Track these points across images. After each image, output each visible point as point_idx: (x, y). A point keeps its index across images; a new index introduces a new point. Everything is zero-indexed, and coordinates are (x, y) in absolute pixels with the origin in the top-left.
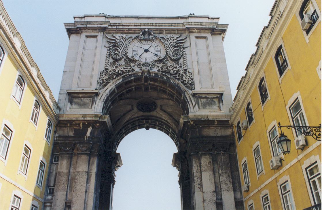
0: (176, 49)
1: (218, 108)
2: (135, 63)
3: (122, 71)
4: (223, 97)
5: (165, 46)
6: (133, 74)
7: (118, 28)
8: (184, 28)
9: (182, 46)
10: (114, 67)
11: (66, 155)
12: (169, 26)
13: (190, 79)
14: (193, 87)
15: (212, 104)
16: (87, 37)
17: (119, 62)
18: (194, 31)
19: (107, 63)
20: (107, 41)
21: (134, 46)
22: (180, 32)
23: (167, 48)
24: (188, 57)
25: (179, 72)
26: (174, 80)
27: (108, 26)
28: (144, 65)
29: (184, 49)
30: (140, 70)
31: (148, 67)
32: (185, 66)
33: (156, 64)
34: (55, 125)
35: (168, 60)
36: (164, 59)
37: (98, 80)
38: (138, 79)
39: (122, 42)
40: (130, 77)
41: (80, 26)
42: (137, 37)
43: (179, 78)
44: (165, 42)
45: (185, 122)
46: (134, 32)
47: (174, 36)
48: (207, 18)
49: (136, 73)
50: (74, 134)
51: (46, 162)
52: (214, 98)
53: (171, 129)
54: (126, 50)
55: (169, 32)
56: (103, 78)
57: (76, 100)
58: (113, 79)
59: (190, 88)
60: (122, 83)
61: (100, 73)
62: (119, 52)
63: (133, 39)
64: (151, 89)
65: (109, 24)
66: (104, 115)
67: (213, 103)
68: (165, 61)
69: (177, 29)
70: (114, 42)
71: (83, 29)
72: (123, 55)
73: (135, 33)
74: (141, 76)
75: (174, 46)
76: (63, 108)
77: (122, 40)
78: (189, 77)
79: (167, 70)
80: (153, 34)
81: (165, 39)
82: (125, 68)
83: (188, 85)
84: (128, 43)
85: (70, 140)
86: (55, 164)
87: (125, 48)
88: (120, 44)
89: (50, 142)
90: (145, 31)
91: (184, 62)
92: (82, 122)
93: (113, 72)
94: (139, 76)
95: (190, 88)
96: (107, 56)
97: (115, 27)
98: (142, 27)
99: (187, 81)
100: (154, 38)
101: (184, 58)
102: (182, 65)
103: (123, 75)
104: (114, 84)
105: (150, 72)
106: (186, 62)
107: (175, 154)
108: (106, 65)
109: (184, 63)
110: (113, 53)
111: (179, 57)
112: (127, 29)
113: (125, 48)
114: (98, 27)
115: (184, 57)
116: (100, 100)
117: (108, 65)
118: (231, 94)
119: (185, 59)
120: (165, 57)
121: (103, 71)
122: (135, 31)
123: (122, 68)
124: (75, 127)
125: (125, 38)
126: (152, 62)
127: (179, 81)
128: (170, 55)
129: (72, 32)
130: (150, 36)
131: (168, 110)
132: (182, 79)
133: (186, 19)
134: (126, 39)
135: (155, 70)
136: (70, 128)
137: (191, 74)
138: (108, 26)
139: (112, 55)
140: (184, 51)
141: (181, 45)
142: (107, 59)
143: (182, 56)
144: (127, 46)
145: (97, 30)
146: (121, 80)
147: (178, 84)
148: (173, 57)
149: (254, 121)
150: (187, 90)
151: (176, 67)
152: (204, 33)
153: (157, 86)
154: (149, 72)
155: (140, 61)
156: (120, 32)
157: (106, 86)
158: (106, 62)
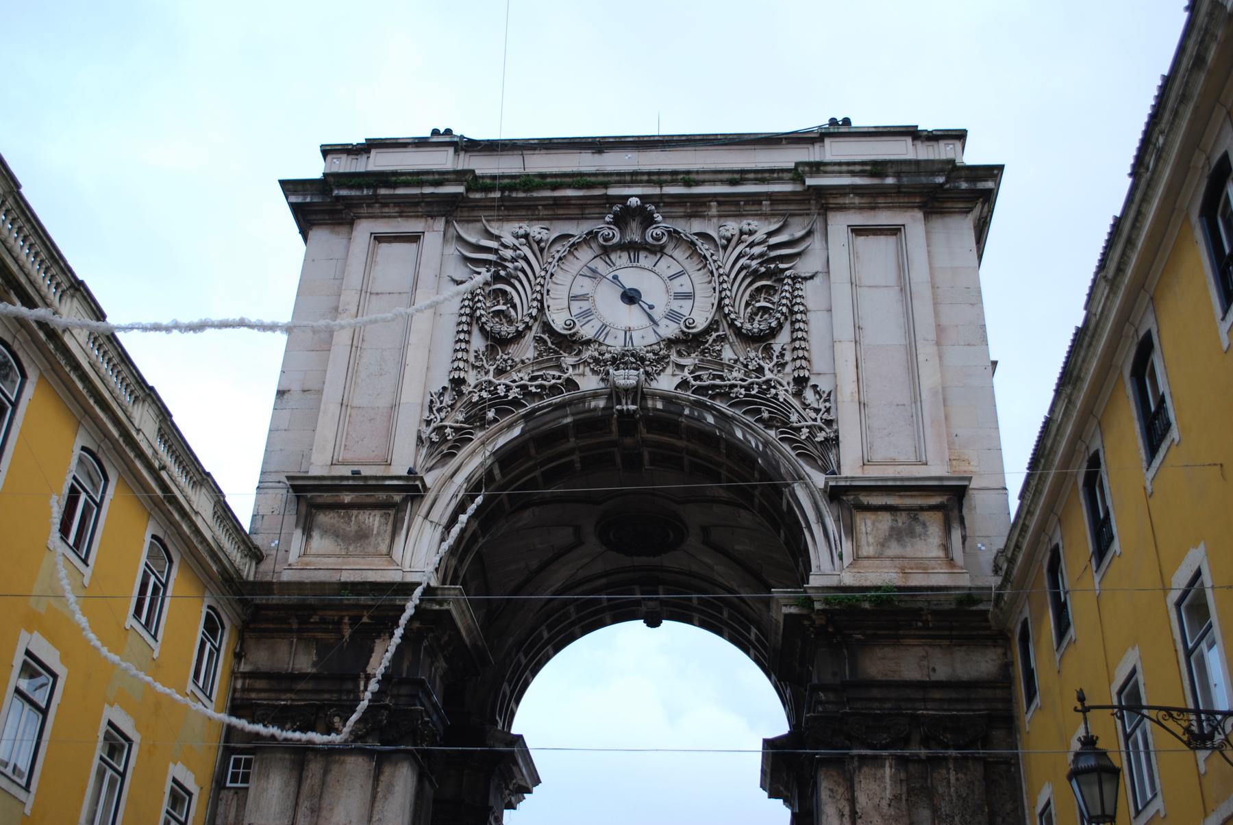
0: (763, 286)
1: (941, 554)
2: (580, 352)
3: (523, 387)
4: (965, 502)
6: (570, 403)
7: (511, 199)
8: (799, 188)
9: (788, 273)
10: (489, 371)
11: (279, 755)
12: (733, 183)
13: (819, 423)
15: (912, 533)
16: (379, 239)
17: (512, 349)
18: (847, 202)
19: (460, 355)
20: (463, 255)
22: (784, 207)
23: (721, 284)
24: (816, 324)
25: (773, 391)
27: (468, 190)
28: (617, 361)
29: (798, 286)
30: (602, 385)
31: (637, 369)
32: (798, 363)
34: (236, 627)
35: (721, 339)
36: (707, 331)
37: (419, 431)
38: (591, 424)
41: (344, 192)
42: (592, 235)
44: (715, 258)
45: (787, 617)
46: (577, 211)
47: (752, 227)
48: (909, 140)
49: (583, 399)
50: (314, 665)
51: (197, 781)
52: (922, 509)
53: (754, 630)
54: (542, 295)
55: (733, 208)
56: (442, 420)
57: (324, 518)
58: (483, 423)
59: (820, 462)
61: (428, 398)
62: (514, 306)
63: (573, 244)
64: (652, 463)
66: (444, 583)
67: (919, 529)
68: (714, 341)
69: (770, 196)
71: (360, 206)
72: (527, 319)
73: (583, 217)
74: (604, 409)
75: (756, 271)
76: (274, 552)
77: (526, 250)
78: (817, 411)
79: (718, 382)
80: (660, 218)
82: (536, 374)
83: (811, 448)
84: (550, 263)
85: (299, 691)
86: (236, 793)
87: (538, 288)
88: (516, 269)
89: (214, 698)
91: (797, 344)
92: (351, 613)
93: (484, 394)
94: (595, 409)
95: (820, 462)
96: (459, 324)
98: (613, 191)
100: (665, 239)
102: (788, 357)
103: (530, 407)
105: (642, 391)
106: (803, 344)
107: (768, 743)
109: (795, 349)
110: (486, 307)
111: (773, 325)
113: (538, 288)
115: (799, 321)
116: (426, 517)
117: (466, 361)
118: (1006, 489)
119: (800, 329)
120: (711, 324)
121: (444, 389)
123: (523, 376)
124: (319, 635)
126: (656, 347)
127: (772, 433)
128: (733, 316)
129: (314, 217)
130: (649, 231)
131: (737, 547)
132: (785, 424)
133: (810, 147)
134: (543, 244)
135: (666, 382)
136: (299, 639)
137: (825, 401)
139: (484, 319)
140: (796, 293)
141: (782, 266)
142: (462, 336)
144: (548, 276)
146: (517, 431)
148: (748, 326)
149: (1072, 631)
151: (760, 370)
152: (893, 207)
154: (636, 393)
155: (600, 344)
157: (454, 455)
158: (456, 351)
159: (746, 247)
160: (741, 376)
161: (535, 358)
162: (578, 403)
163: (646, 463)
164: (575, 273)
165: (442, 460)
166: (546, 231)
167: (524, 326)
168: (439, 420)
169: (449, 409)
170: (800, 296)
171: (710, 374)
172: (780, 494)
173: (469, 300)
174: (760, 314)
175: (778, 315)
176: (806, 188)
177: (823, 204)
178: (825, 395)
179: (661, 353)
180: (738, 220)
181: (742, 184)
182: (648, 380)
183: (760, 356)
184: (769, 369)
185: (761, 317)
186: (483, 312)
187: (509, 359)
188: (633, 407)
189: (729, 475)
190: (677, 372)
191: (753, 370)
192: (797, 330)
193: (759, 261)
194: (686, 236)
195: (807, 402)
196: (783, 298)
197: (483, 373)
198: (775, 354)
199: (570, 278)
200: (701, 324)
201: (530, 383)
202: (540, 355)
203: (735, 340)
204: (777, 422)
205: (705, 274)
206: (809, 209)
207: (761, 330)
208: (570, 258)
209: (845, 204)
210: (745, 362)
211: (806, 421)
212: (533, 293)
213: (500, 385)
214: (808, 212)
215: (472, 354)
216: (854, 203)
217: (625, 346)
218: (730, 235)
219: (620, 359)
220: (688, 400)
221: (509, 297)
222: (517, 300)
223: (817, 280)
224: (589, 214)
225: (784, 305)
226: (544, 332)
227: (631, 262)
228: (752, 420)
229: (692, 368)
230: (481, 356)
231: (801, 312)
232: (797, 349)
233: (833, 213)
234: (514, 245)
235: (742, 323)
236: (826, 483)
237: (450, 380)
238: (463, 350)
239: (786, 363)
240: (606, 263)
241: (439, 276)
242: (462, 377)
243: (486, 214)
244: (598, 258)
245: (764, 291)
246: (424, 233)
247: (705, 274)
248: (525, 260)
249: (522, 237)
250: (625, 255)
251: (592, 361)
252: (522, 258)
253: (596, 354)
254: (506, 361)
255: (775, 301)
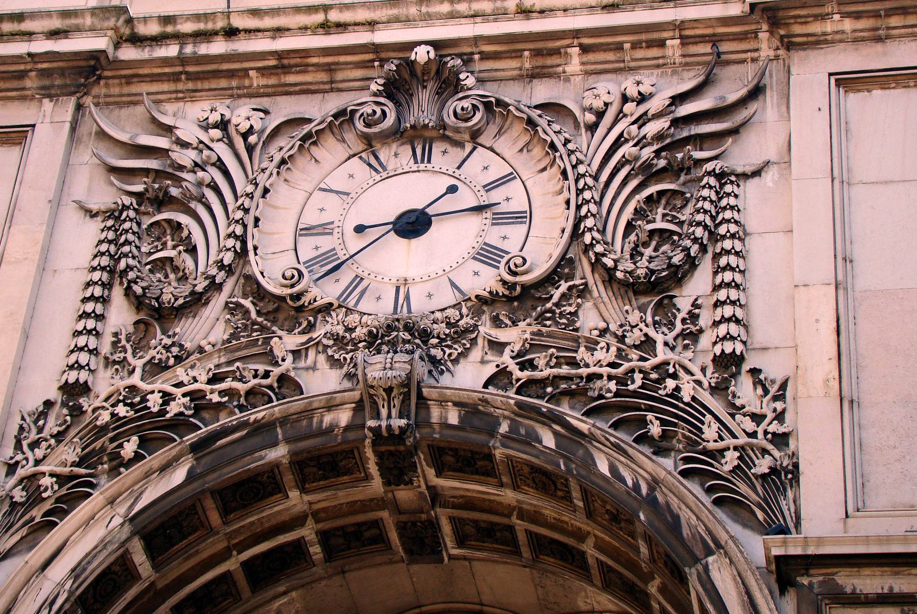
0: (661, 193)
2: (311, 327)
3: (197, 396)
5: (564, 173)
6: (284, 420)
9: (709, 166)
13: (761, 441)
14: (786, 505)
18: (829, 27)
19: (82, 341)
21: (318, 195)
23: (579, 192)
25: (671, 384)
26: (624, 453)
27: (117, 46)
29: (728, 188)
30: (347, 384)
32: (722, 330)
33: (486, 329)
36: (551, 279)
39: (220, 165)
40: (257, 440)
42: (344, 117)
43: (665, 435)
44: (571, 146)
46: (323, 76)
47: (645, 89)
49: (308, 412)
54: (245, 226)
55: (610, 56)
56: (37, 462)
58: (118, 464)
59: (760, 515)
60: (198, 497)
62: (192, 250)
65: (126, 31)
68: (563, 295)
69: (679, 26)
70: (158, 174)
72: (213, 271)
73: (332, 87)
74: (347, 428)
75: (647, 166)
77: (222, 150)
78: (757, 418)
79: (565, 370)
81: (575, 119)
83: (744, 488)
84: (263, 170)
87: (239, 215)
88: (200, 184)
90: (411, 64)
91: (722, 295)
93: (122, 410)
95: (760, 515)
97: (171, 50)
98: (383, 36)
99: (731, 458)
100: (478, 116)
101: (723, 261)
102: (705, 320)
103: (204, 430)
104: (122, 510)
105: (420, 396)
108: (72, 359)
109: (718, 304)
111: (676, 260)
112: (262, 55)
113: (239, 215)
114: (30, 55)
115: (728, 252)
117: (94, 352)
119: (728, 267)
120: (559, 265)
121: (48, 404)
122: (330, 68)
125: (245, 136)
126: (453, 313)
127: (668, 462)
128: (599, 248)
132: (692, 444)
137: (775, 398)
138: (117, 46)
139: (132, 275)
140: (724, 202)
142: (89, 307)
143: (703, 249)
144: (259, 193)
145: (28, 83)
146: (179, 476)
147: (652, 489)
148: (630, 266)
150: (723, 537)
151: (647, 344)
153: (508, 509)
155: (349, 311)
156: (214, 84)
159: (633, 123)
160: (611, 356)
161: (224, 342)
162: (298, 421)
163: (449, 544)
164: (309, 187)
165: (30, 537)
166: (262, 115)
167: (207, 282)
168: (31, 462)
169: (53, 441)
170: (732, 208)
171: (552, 355)
172: (683, 580)
173: (110, 242)
174: (654, 243)
175: (688, 243)
176: (747, 9)
177: (782, 37)
178: (776, 387)
179: (461, 323)
180: (620, 77)
181: (624, 10)
182: (435, 373)
183: (649, 319)
184: (666, 344)
185: (656, 250)
186: (131, 262)
187: (173, 344)
188: (398, 423)
189: (603, 558)
190: (489, 357)
191: (636, 347)
192: (724, 269)
193: (655, 147)
194: (518, 109)
195: (738, 402)
196: (698, 211)
197: (126, 373)
198: (680, 316)
199: (301, 196)
200: (540, 266)
201: (209, 387)
202: (234, 336)
203: (604, 294)
204: (679, 441)
205: (549, 180)
206: (757, 50)
207: (652, 272)
208: (302, 161)
209: (825, 34)
210: (620, 333)
211: (734, 436)
212: (229, 225)
213: (153, 392)
214: (755, 55)
215: (108, 339)
216: (843, 32)
217: (395, 311)
218: (601, 105)
219: (383, 336)
220: (507, 407)
221: (185, 234)
222: (198, 238)
223: (770, 177)
224: (344, 81)
225: (699, 224)
226: (245, 296)
227: (416, 162)
228: (629, 439)
229: (517, 348)
230: (124, 342)
231: (733, 236)
232: (724, 303)
233: (802, 53)
234: (201, 142)
235: (615, 261)
236: (767, 550)
237: (60, 388)
238: (89, 332)
239: (701, 331)
240: (370, 165)
241: (56, 204)
242: (82, 381)
243: (155, 87)
244: (356, 159)
245: (663, 202)
246: (34, 126)
247: (549, 180)
248: (219, 168)
249: (216, 126)
250: (406, 151)
251: (331, 342)
252: (213, 165)
253: (340, 330)
254: (167, 348)
255: (683, 218)
